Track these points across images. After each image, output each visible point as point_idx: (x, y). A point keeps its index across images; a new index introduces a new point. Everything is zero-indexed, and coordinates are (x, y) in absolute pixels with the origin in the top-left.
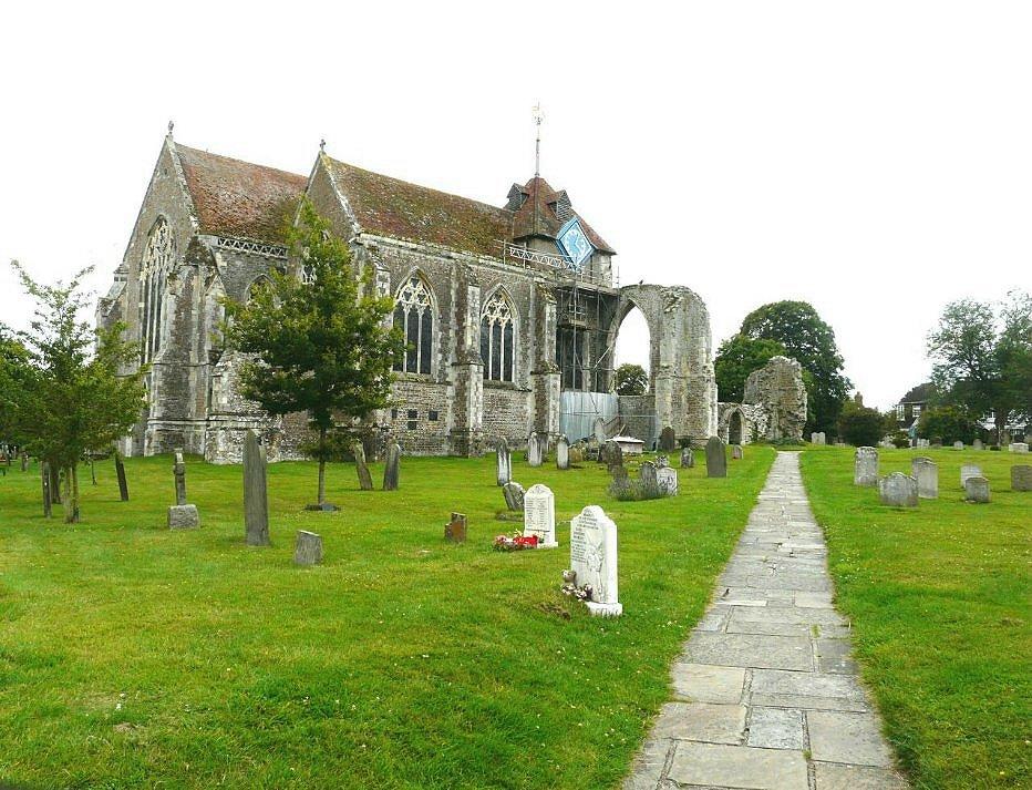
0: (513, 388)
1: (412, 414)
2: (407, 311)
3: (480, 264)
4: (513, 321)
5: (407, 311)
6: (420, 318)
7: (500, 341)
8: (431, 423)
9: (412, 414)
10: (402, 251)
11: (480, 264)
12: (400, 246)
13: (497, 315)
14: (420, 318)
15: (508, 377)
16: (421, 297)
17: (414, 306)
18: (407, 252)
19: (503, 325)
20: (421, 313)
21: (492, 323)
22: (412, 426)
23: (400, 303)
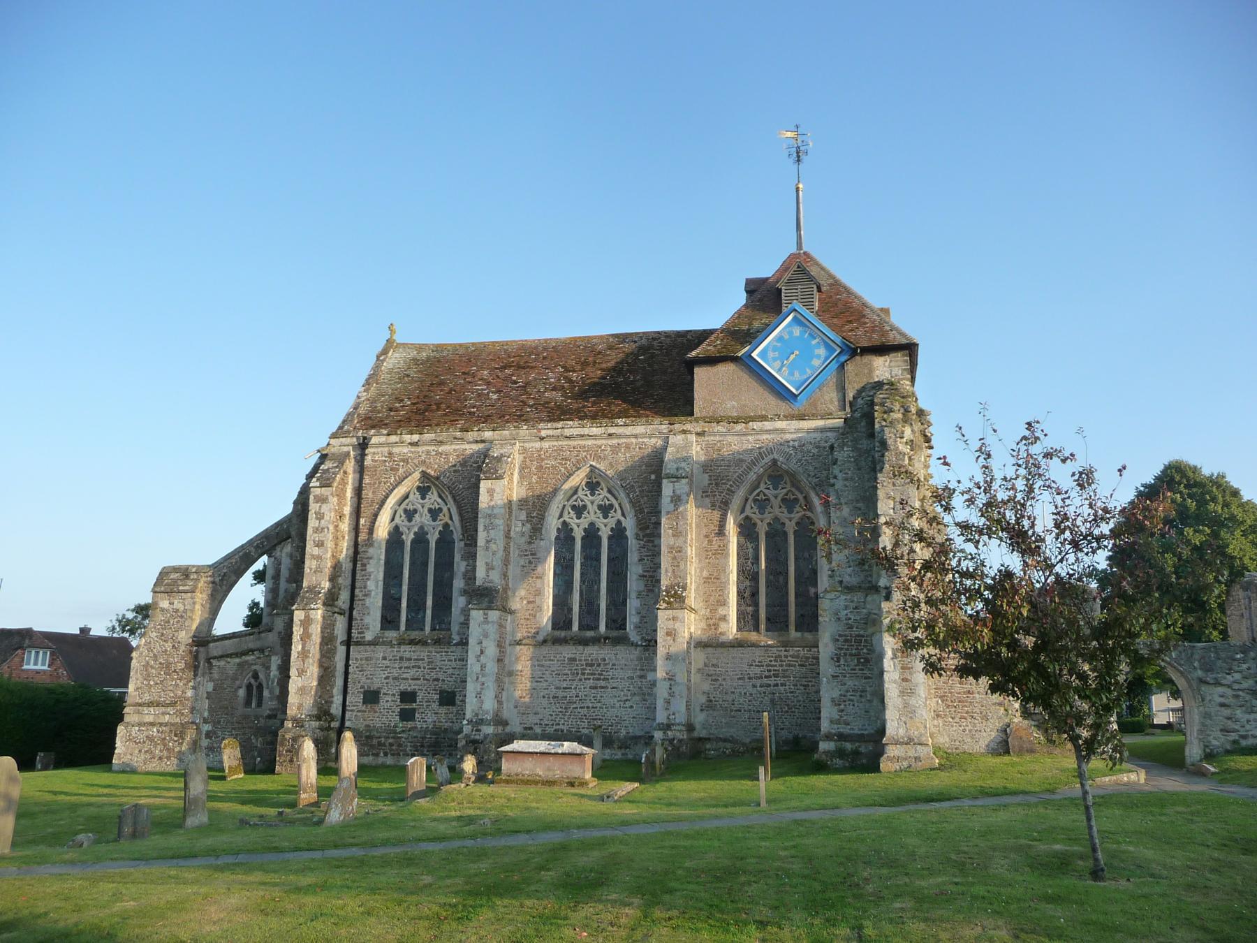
0: (622, 640)
1: (408, 697)
2: (408, 538)
3: (542, 439)
4: (625, 523)
5: (408, 538)
6: (433, 545)
7: (598, 559)
8: (443, 710)
9: (408, 697)
10: (396, 450)
11: (542, 439)
12: (389, 445)
13: (593, 515)
14: (433, 545)
15: (617, 622)
16: (434, 513)
17: (421, 528)
18: (405, 450)
19: (605, 533)
20: (433, 538)
21: (578, 534)
22: (406, 715)
23: (397, 528)
